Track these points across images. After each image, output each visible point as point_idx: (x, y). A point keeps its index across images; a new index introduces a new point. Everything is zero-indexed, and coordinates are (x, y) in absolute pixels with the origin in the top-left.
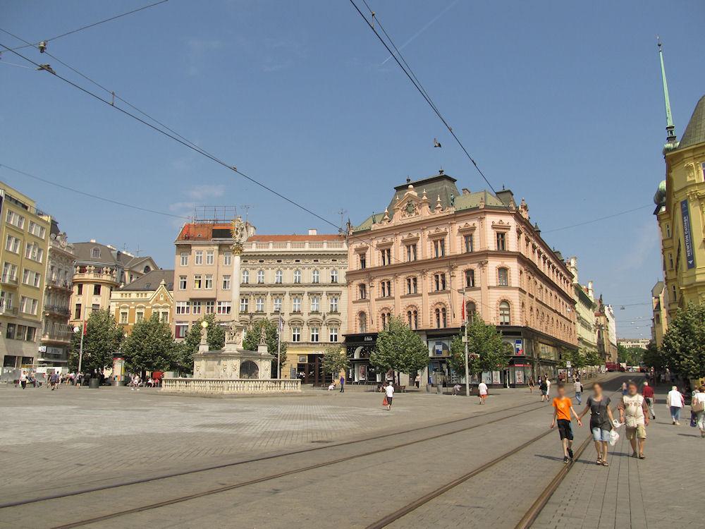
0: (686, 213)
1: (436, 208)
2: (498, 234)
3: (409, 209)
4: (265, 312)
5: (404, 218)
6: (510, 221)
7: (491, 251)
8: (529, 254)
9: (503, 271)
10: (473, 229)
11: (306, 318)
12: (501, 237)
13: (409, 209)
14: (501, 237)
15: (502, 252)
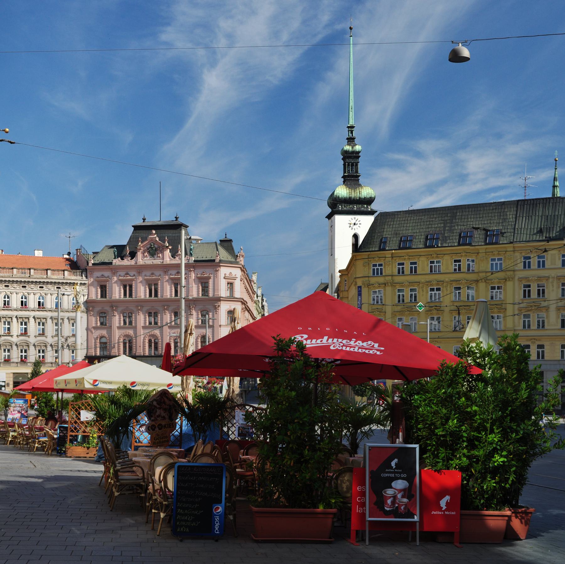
0: (360, 294)
1: (177, 256)
2: (228, 283)
3: (153, 251)
4: (11, 334)
5: (145, 259)
6: (237, 272)
7: (223, 298)
8: (246, 298)
9: (231, 313)
10: (210, 278)
11: (32, 340)
12: (231, 285)
13: (153, 251)
14: (231, 285)
15: (231, 298)
